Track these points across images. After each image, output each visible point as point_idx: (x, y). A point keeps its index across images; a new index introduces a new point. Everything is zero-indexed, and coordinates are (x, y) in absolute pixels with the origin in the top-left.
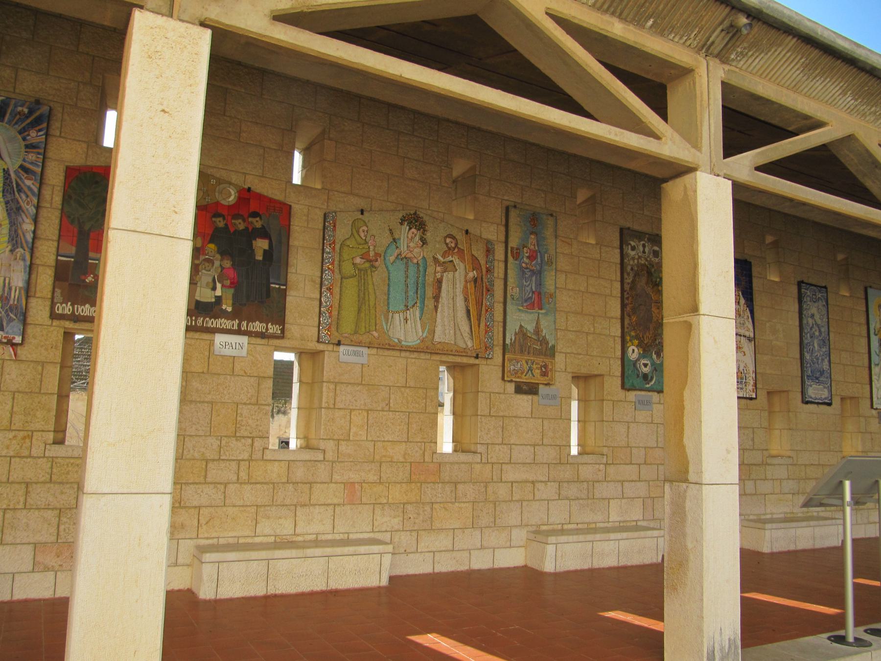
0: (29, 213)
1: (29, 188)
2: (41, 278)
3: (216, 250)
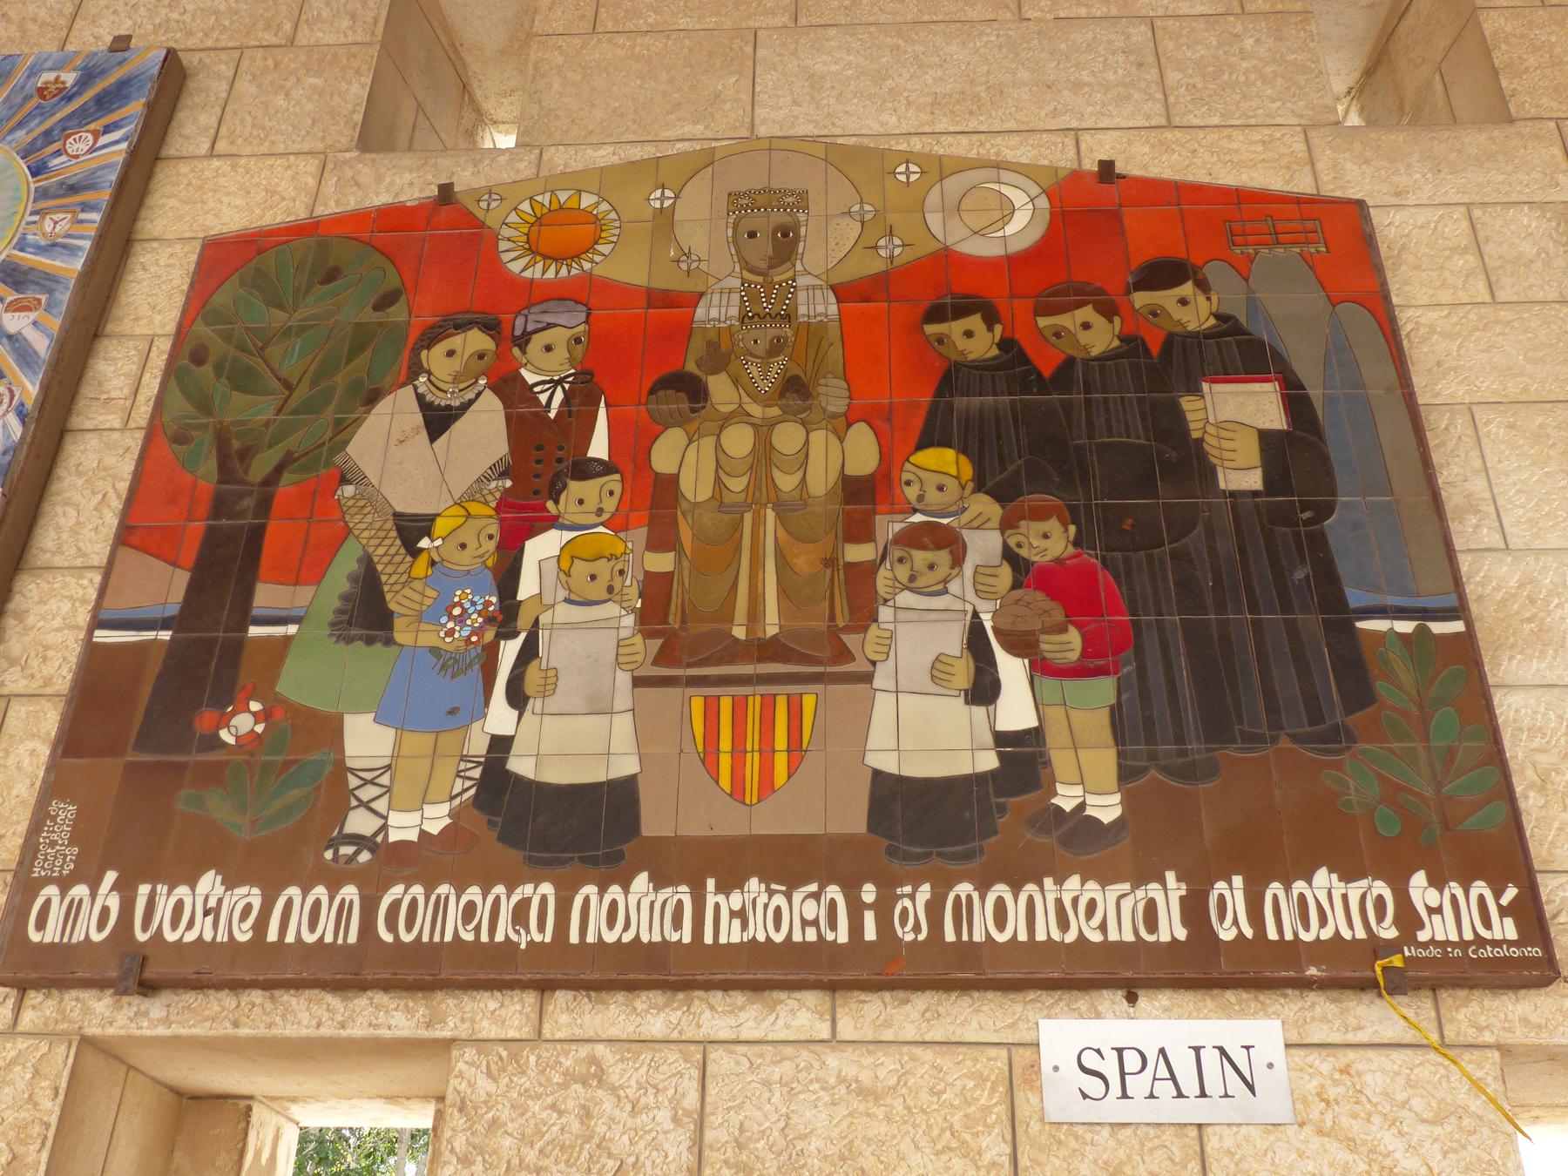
3: (967, 470)
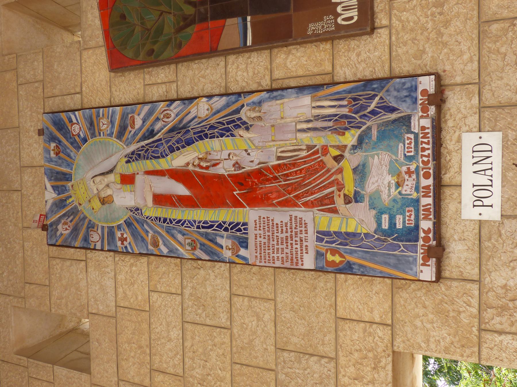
0: (181, 111)
1: (144, 121)
2: (294, 69)
